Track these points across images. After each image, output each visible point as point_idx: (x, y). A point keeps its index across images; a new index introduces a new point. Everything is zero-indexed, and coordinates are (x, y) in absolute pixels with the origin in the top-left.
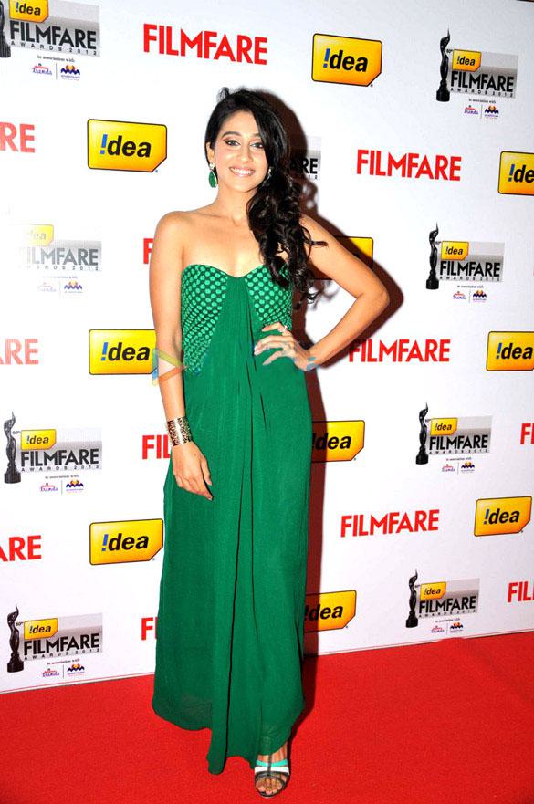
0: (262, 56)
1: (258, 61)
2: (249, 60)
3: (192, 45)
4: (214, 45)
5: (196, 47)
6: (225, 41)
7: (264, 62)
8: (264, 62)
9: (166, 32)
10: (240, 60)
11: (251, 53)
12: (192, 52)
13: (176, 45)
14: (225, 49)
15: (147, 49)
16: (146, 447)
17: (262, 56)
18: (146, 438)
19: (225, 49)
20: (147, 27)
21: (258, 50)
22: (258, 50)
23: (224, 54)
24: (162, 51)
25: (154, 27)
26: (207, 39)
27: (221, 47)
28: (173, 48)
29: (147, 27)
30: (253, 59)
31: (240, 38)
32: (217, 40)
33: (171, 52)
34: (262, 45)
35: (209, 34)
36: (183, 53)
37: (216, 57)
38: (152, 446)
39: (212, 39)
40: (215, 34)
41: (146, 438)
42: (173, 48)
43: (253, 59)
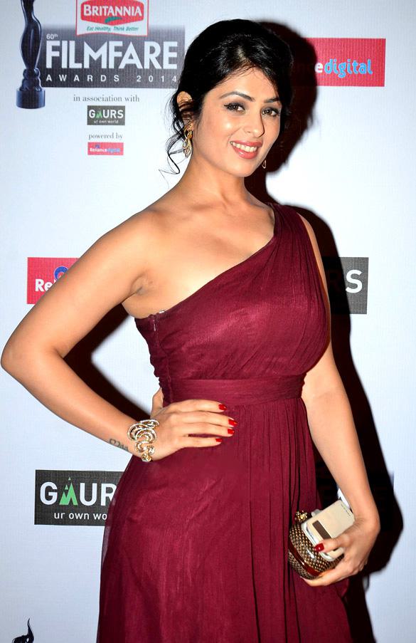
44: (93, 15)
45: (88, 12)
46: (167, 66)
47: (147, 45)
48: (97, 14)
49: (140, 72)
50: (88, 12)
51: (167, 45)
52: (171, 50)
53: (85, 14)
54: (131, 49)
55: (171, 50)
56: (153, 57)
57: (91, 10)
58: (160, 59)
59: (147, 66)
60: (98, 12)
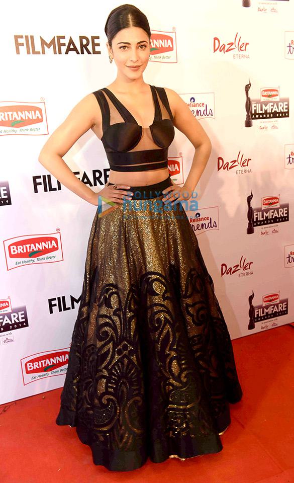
0: (97, 49)
1: (95, 52)
2: (89, 53)
3: (49, 46)
4: (64, 45)
5: (52, 46)
6: (71, 42)
7: (99, 53)
8: (99, 53)
9: (30, 40)
10: (83, 53)
11: (90, 47)
12: (49, 51)
13: (38, 47)
14: (72, 47)
15: (18, 52)
16: (51, 306)
17: (97, 49)
18: (50, 301)
19: (72, 47)
20: (17, 37)
21: (94, 45)
22: (94, 45)
23: (72, 50)
24: (28, 53)
25: (22, 37)
26: (59, 41)
27: (69, 45)
28: (36, 50)
29: (17, 37)
30: (91, 51)
31: (81, 38)
32: (66, 41)
33: (35, 53)
34: (96, 41)
35: (59, 38)
36: (44, 53)
37: (67, 53)
38: (55, 305)
39: (62, 41)
40: (64, 37)
41: (50, 301)
42: (37, 50)
43: (92, 52)
44: (19, 252)
45: (14, 251)
46: (21, 320)
47: (12, 315)
48: (22, 252)
49: (11, 325)
50: (14, 251)
51: (20, 313)
52: (22, 314)
53: (13, 253)
54: (6, 318)
55: (22, 314)
56: (15, 319)
57: (17, 249)
58: (18, 319)
59: (13, 322)
60: (23, 250)
